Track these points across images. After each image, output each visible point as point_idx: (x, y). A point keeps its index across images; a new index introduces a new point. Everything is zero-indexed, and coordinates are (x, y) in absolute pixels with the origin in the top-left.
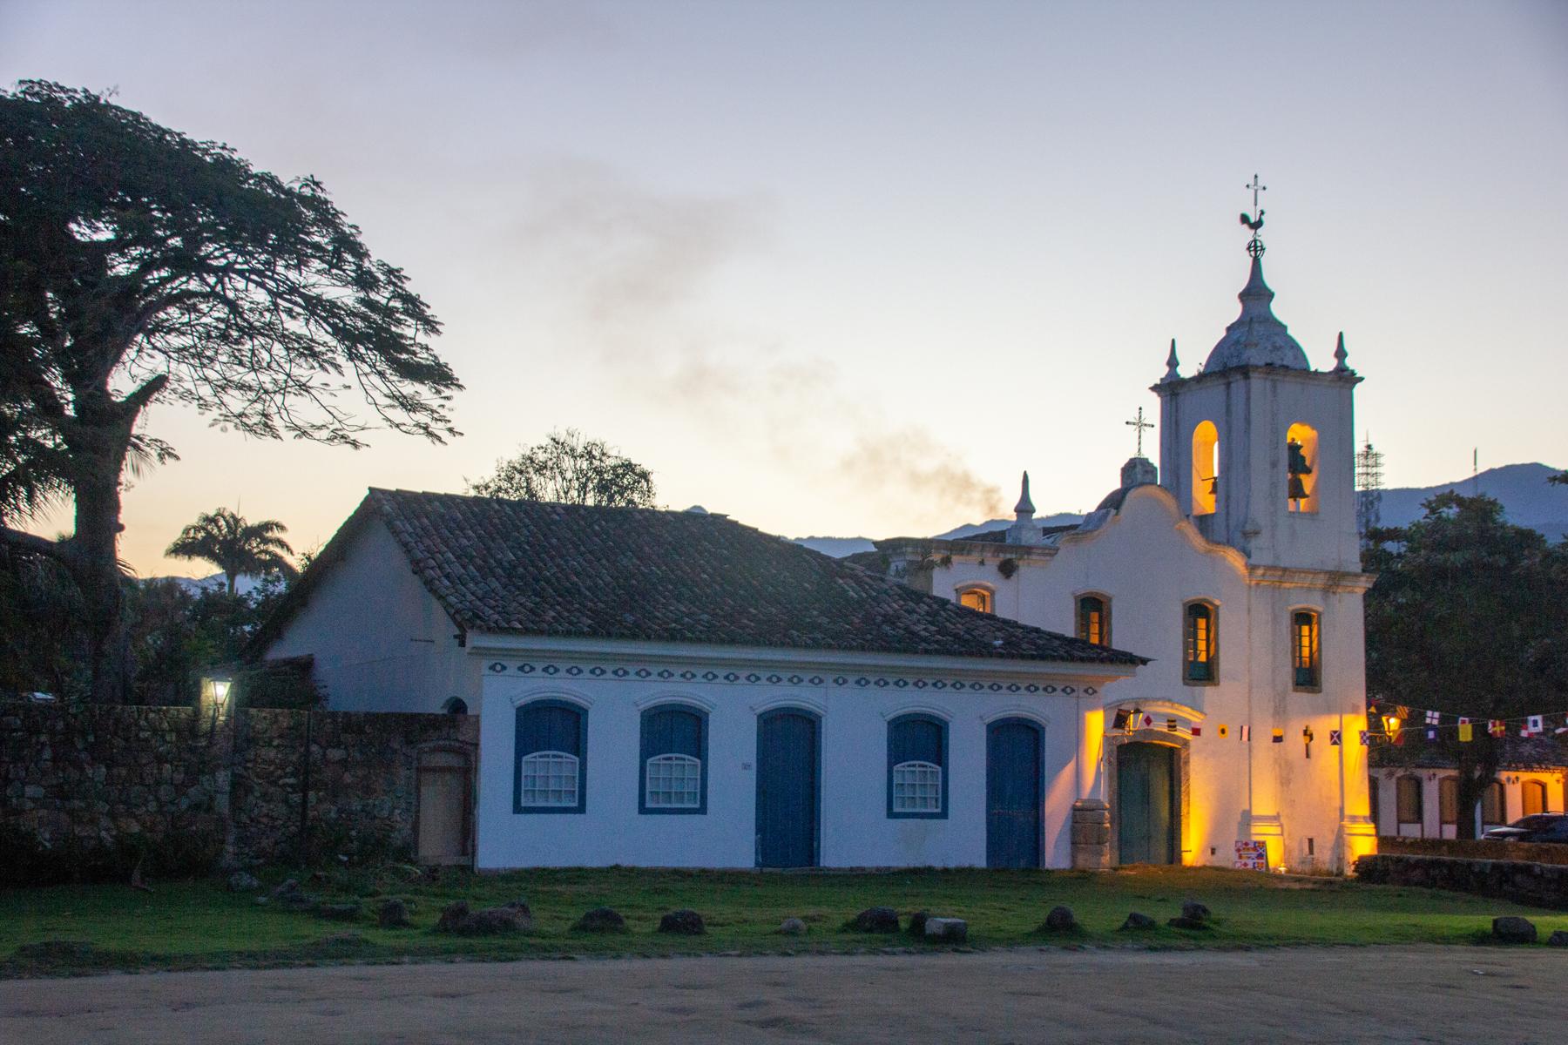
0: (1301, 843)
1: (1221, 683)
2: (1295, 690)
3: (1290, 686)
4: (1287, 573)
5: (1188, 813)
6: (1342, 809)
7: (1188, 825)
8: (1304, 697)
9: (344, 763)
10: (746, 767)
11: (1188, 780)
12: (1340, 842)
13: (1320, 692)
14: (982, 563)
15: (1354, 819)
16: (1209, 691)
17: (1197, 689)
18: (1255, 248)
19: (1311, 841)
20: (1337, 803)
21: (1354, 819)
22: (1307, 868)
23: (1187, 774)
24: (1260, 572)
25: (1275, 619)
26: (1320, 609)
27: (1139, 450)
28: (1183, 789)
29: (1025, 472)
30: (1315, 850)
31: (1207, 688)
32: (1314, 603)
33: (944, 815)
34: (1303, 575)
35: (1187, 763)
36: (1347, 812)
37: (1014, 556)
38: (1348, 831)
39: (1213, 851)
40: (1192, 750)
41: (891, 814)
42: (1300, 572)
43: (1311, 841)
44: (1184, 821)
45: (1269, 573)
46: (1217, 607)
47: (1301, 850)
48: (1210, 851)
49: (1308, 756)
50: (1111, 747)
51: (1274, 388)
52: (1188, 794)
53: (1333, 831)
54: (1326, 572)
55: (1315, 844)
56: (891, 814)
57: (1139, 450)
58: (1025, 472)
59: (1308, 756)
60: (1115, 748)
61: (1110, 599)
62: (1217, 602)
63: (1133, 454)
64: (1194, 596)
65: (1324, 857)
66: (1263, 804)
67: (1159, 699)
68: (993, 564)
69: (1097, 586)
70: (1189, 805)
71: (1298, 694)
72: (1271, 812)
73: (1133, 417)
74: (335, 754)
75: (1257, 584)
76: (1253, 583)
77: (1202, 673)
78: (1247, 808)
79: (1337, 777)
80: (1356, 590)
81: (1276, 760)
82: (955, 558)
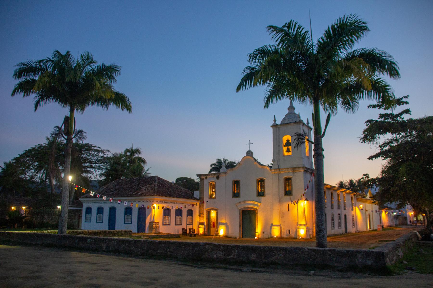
0: (286, 231)
1: (266, 196)
2: (285, 196)
3: (284, 194)
4: (280, 170)
5: (258, 224)
6: (298, 223)
7: (257, 227)
8: (288, 197)
9: (73, 216)
10: (108, 216)
11: (257, 217)
12: (296, 232)
13: (292, 196)
14: (213, 177)
15: (301, 225)
16: (263, 198)
17: (260, 198)
19: (289, 230)
20: (297, 222)
21: (301, 225)
22: (288, 237)
23: (257, 216)
24: (273, 170)
25: (279, 180)
26: (291, 177)
28: (256, 219)
30: (290, 233)
31: (262, 197)
32: (290, 176)
33: (131, 224)
34: (285, 170)
35: (257, 213)
36: (299, 224)
37: (218, 175)
38: (298, 228)
39: (263, 233)
40: (258, 211)
41: (125, 223)
42: (284, 169)
43: (289, 230)
44: (256, 226)
45: (275, 170)
46: (265, 179)
47: (286, 232)
48: (262, 233)
49: (289, 211)
51: (279, 129)
52: (257, 220)
53: (295, 228)
54: (291, 168)
55: (290, 231)
56: (125, 223)
59: (289, 211)
60: (241, 212)
61: (240, 181)
62: (264, 178)
63: (248, 150)
64: (260, 177)
65: (293, 235)
66: (276, 222)
67: (248, 200)
68: (215, 176)
69: (237, 179)
70: (258, 222)
71: (286, 197)
72: (278, 224)
73: (248, 143)
74: (72, 214)
75: (274, 173)
76: (273, 173)
77: (261, 194)
78: (272, 223)
79: (297, 215)
80: (301, 171)
81: (280, 212)
82: (208, 177)
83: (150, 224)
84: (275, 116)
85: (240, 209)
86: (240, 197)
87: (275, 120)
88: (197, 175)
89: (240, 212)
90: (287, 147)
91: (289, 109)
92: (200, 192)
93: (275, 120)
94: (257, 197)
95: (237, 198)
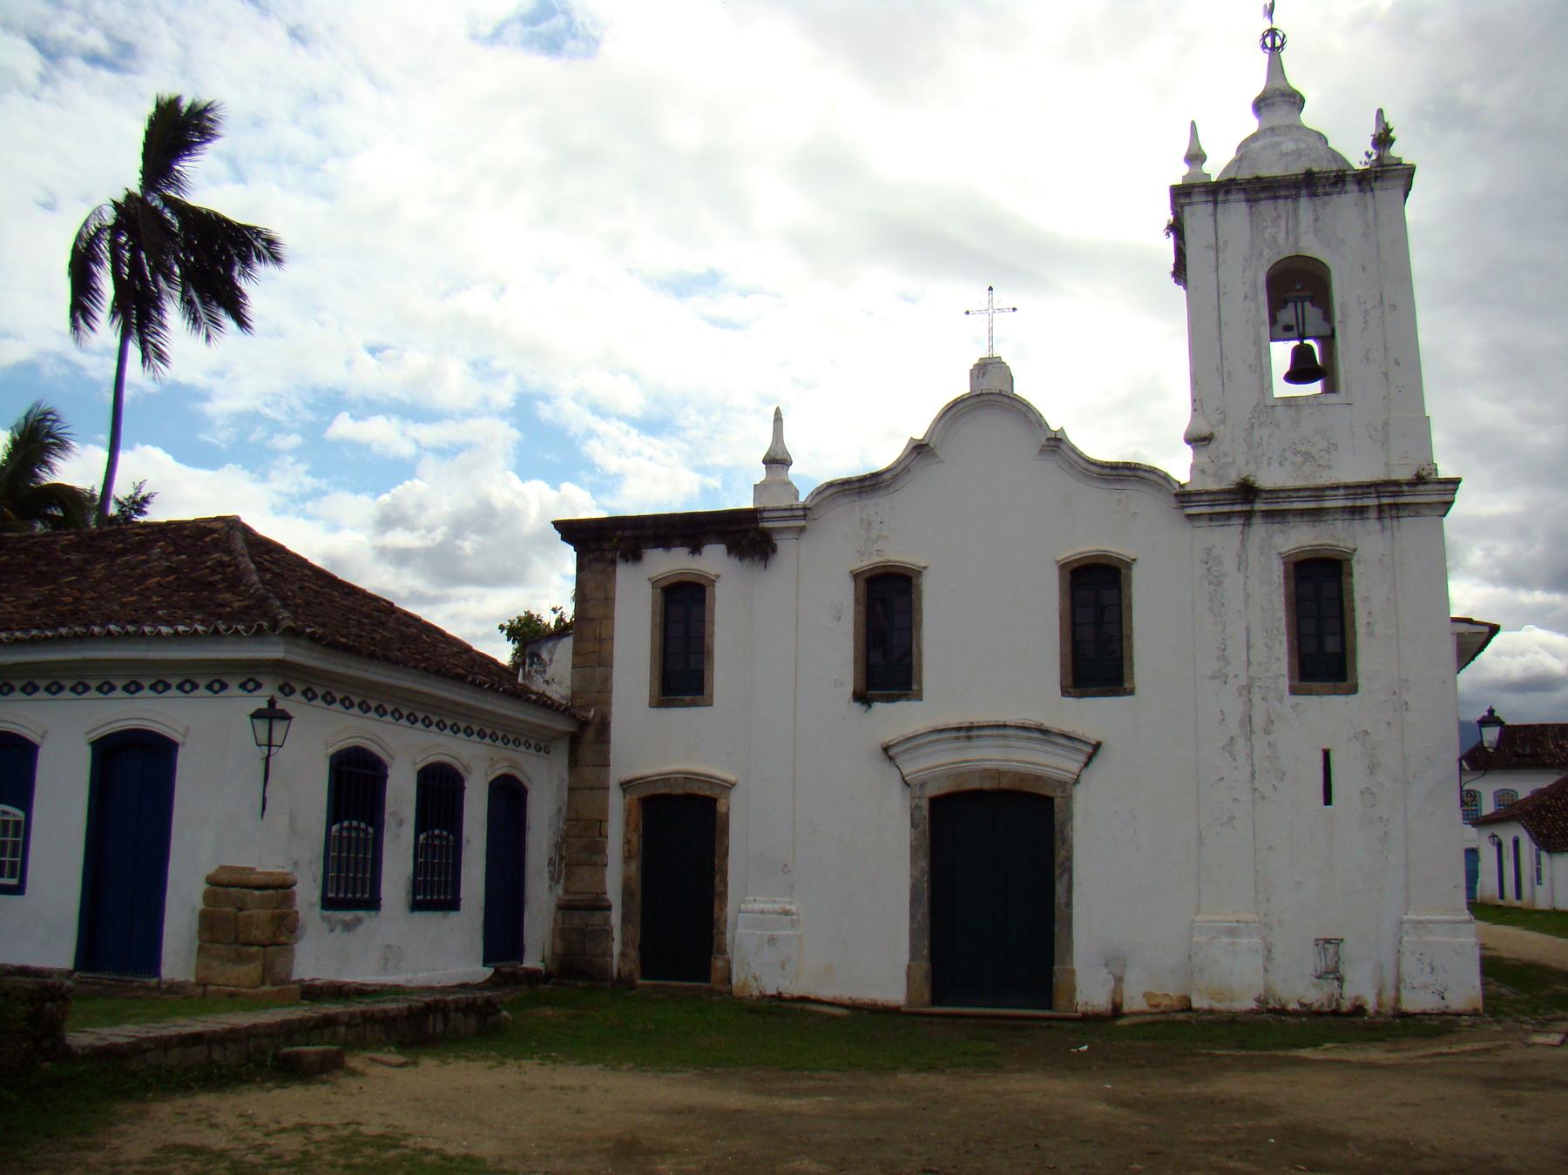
18: (1273, 43)
27: (991, 347)
29: (778, 408)
49: (1328, 800)
50: (917, 801)
57: (991, 347)
58: (778, 408)
59: (1328, 800)
60: (925, 804)
61: (918, 573)
83: (208, 897)
84: (1193, 125)
85: (922, 785)
86: (919, 697)
87: (1195, 157)
88: (559, 525)
89: (915, 809)
90: (1297, 343)
91: (1260, 105)
92: (577, 653)
93: (1195, 157)
94: (1065, 692)
95: (901, 706)
